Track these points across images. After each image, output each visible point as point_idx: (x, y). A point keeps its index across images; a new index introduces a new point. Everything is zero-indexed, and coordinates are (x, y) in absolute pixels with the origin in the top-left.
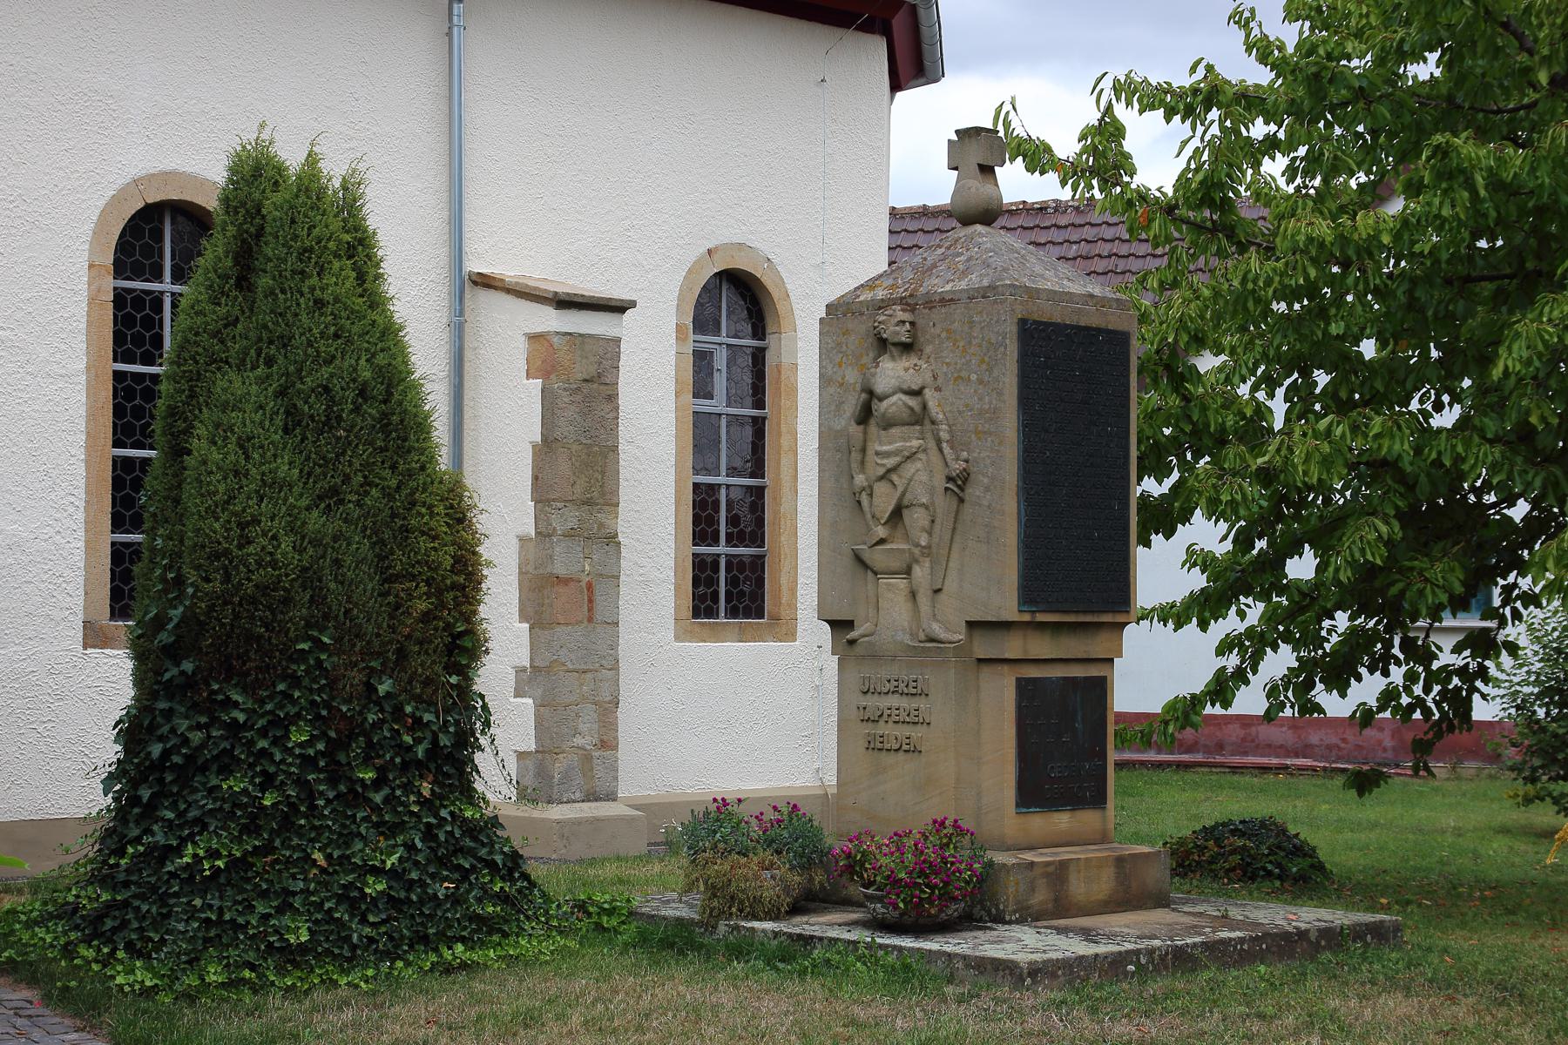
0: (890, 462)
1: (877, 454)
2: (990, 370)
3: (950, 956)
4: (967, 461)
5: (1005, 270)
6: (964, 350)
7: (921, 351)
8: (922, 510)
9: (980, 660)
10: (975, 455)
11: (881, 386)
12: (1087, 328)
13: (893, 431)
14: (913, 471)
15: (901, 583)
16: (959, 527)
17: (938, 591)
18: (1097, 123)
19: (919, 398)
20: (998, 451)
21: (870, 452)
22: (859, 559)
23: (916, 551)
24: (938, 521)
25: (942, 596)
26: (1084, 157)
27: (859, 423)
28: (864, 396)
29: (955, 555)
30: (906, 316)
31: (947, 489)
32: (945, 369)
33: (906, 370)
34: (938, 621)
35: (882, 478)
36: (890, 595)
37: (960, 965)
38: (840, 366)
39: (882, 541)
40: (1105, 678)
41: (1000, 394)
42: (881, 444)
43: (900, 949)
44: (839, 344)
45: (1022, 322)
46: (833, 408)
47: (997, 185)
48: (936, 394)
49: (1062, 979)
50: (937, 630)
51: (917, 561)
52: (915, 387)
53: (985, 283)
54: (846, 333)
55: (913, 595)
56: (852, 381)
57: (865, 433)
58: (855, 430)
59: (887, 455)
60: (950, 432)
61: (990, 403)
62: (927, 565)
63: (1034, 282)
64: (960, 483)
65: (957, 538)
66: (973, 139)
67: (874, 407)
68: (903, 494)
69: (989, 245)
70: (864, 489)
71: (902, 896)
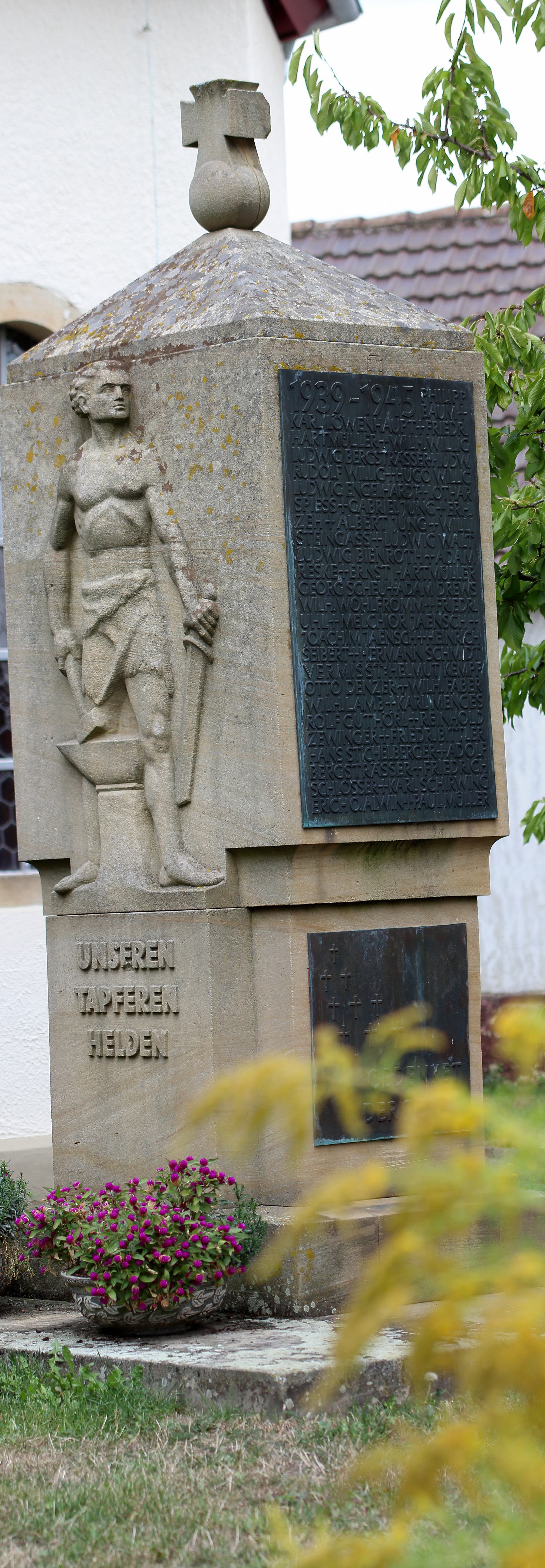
0: (103, 606)
1: (85, 594)
2: (239, 453)
3: (178, 1370)
4: (213, 598)
5: (258, 296)
6: (202, 425)
7: (142, 428)
8: (153, 679)
9: (252, 910)
10: (225, 587)
11: (83, 490)
12: (398, 381)
13: (106, 557)
14: (136, 618)
15: (129, 796)
16: (208, 700)
17: (184, 805)
18: (447, 67)
19: (140, 504)
20: (258, 579)
21: (77, 593)
22: (71, 765)
23: (149, 744)
24: (178, 695)
25: (191, 813)
26: (433, 118)
27: (59, 548)
28: (62, 504)
29: (205, 746)
30: (117, 377)
31: (187, 643)
32: (176, 455)
33: (120, 460)
34: (186, 852)
35: (93, 632)
36: (116, 817)
37: (192, 1384)
38: (30, 460)
39: (98, 732)
40: (460, 930)
41: (255, 489)
42: (91, 579)
43: (109, 1363)
44: (27, 426)
45: (285, 376)
46: (23, 526)
47: (257, 166)
48: (166, 496)
49: (346, 1398)
50: (186, 868)
51: (151, 760)
52: (133, 487)
53: (228, 318)
54: (36, 407)
55: (148, 812)
56: (47, 482)
57: (69, 563)
58: (55, 559)
59: (97, 595)
60: (188, 553)
61: (242, 504)
62: (166, 764)
63: (305, 312)
64: (204, 632)
65: (207, 719)
66: (217, 99)
67: (78, 522)
68: (125, 656)
69: (240, 260)
70: (69, 652)
71: (114, 1282)
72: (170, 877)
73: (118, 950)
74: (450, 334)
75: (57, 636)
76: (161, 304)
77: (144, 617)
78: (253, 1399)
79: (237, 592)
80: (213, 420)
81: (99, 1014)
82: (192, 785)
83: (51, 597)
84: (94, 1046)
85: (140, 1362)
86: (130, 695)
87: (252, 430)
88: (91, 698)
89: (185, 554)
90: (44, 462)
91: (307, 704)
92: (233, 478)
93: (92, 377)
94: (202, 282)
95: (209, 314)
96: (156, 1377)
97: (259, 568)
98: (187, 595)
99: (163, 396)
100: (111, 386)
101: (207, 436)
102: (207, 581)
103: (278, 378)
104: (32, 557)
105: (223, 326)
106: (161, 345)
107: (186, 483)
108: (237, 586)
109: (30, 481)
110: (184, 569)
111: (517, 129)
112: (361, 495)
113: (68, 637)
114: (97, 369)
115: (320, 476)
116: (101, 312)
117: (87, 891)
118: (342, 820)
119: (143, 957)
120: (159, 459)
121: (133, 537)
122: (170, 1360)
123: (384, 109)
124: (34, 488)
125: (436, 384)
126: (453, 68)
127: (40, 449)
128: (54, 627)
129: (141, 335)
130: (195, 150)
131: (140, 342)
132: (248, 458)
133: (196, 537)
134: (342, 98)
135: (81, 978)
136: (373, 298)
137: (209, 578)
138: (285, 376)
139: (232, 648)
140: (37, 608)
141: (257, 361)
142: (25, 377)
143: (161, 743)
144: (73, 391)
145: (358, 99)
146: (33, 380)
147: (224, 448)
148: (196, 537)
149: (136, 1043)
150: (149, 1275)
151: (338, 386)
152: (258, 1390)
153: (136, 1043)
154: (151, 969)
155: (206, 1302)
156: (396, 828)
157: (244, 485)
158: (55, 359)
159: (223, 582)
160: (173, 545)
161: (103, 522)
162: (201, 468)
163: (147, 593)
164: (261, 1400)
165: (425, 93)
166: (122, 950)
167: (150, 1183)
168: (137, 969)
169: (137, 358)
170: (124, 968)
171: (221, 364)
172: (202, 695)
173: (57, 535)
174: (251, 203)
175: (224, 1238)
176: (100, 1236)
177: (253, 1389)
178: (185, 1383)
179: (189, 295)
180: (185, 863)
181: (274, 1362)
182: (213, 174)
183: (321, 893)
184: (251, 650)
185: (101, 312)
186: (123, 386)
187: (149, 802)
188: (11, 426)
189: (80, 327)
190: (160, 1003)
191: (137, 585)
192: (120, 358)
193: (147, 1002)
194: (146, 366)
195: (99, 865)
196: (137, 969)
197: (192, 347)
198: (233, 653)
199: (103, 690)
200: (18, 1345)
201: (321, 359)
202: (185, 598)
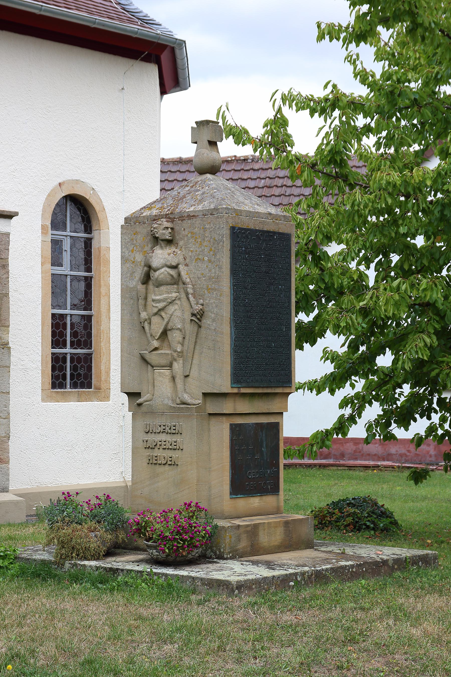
0: (161, 305)
1: (153, 300)
2: (215, 255)
3: (193, 578)
4: (202, 305)
5: (223, 199)
6: (201, 244)
7: (177, 244)
8: (178, 332)
9: (210, 414)
10: (207, 301)
11: (155, 263)
12: (268, 232)
13: (163, 288)
14: (173, 310)
15: (167, 372)
16: (198, 340)
17: (187, 376)
18: (273, 118)
19: (176, 270)
20: (220, 299)
21: (149, 300)
22: (143, 359)
23: (175, 354)
24: (187, 338)
25: (189, 379)
26: (266, 136)
27: (143, 283)
28: (146, 268)
29: (196, 356)
30: (169, 225)
31: (192, 320)
32: (190, 254)
33: (169, 254)
34: (187, 393)
35: (156, 314)
36: (161, 379)
37: (199, 584)
38: (133, 252)
39: (156, 349)
40: (279, 423)
41: (220, 268)
42: (155, 295)
43: (166, 575)
44: (132, 240)
45: (233, 228)
46: (129, 275)
47: (218, 152)
48: (186, 268)
49: (255, 590)
50: (187, 398)
51: (175, 360)
52: (174, 264)
53: (212, 207)
54: (136, 233)
55: (173, 378)
56: (139, 260)
57: (147, 289)
58: (141, 288)
59: (159, 301)
60: (193, 289)
61: (215, 273)
62: (181, 362)
63: (239, 206)
64: (199, 317)
65: (197, 347)
66: (205, 127)
67: (151, 275)
68: (168, 323)
69: (214, 186)
70: (146, 320)
71: (167, 546)
72: (181, 401)
73: (160, 426)
74: (284, 216)
75: (142, 314)
76: (184, 200)
77: (176, 310)
78: (223, 590)
79: (212, 303)
80: (205, 242)
81: (152, 448)
82: (190, 370)
83: (140, 301)
84: (149, 460)
85: (178, 575)
86: (169, 336)
87: (220, 247)
88: (154, 337)
89: (192, 289)
90: (138, 253)
91: (235, 344)
92: (212, 263)
93: (160, 224)
94: (199, 193)
95: (204, 205)
96: (185, 581)
97: (220, 295)
98: (193, 303)
99: (186, 232)
100: (167, 228)
101: (203, 248)
102: (200, 299)
103: (230, 229)
104: (132, 286)
105: (210, 209)
106: (186, 215)
107: (194, 264)
108: (212, 301)
109: (132, 259)
110: (192, 294)
111: (295, 142)
112: (255, 272)
113: (145, 315)
114: (162, 222)
115: (242, 264)
116: (160, 201)
117: (149, 404)
118: (244, 385)
119: (170, 429)
120: (183, 255)
121: (173, 282)
122: (190, 574)
123: (249, 132)
124: (134, 262)
125: (280, 234)
126: (275, 118)
127: (137, 248)
128: (140, 311)
129: (178, 210)
130: (196, 145)
131: (177, 213)
132: (218, 257)
133: (196, 283)
134: (234, 127)
135: (145, 435)
136: (258, 202)
137: (201, 298)
138: (233, 228)
139: (208, 323)
140: (133, 304)
141: (223, 223)
142: (131, 222)
143: (180, 354)
144: (152, 229)
145: (240, 128)
146: (135, 224)
147: (209, 253)
148: (196, 283)
149: (166, 459)
150: (180, 543)
151: (249, 233)
152: (225, 587)
153: (166, 459)
154: (173, 433)
155: (196, 553)
156: (260, 388)
157: (216, 266)
158: (144, 217)
159: (206, 300)
160: (188, 285)
161: (162, 276)
162: (200, 259)
163: (177, 302)
164: (226, 590)
165: (264, 127)
166: (162, 426)
167: (177, 510)
168: (167, 433)
169: (177, 219)
170: (162, 432)
171: (209, 223)
172: (196, 339)
173: (143, 279)
174: (216, 165)
175: (204, 531)
176: (162, 529)
177: (223, 586)
178: (196, 583)
179: (195, 197)
180: (187, 397)
181: (228, 576)
182: (203, 154)
183: (235, 409)
184: (216, 324)
185: (160, 201)
186: (171, 228)
187: (174, 374)
188: (126, 239)
189: (153, 205)
190: (176, 445)
191: (174, 299)
192: (169, 218)
193: (171, 445)
194: (180, 222)
195: (153, 395)
196: (167, 433)
197: (198, 216)
198: (209, 325)
199: (159, 334)
200: (129, 567)
201: (244, 223)
202: (192, 304)
